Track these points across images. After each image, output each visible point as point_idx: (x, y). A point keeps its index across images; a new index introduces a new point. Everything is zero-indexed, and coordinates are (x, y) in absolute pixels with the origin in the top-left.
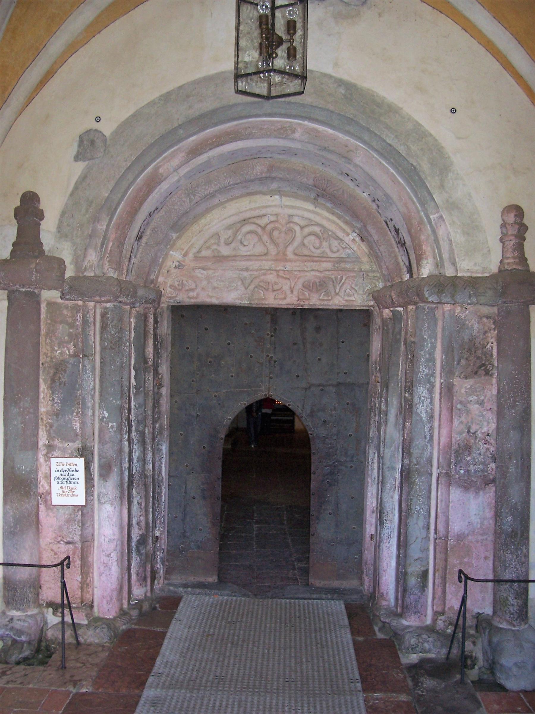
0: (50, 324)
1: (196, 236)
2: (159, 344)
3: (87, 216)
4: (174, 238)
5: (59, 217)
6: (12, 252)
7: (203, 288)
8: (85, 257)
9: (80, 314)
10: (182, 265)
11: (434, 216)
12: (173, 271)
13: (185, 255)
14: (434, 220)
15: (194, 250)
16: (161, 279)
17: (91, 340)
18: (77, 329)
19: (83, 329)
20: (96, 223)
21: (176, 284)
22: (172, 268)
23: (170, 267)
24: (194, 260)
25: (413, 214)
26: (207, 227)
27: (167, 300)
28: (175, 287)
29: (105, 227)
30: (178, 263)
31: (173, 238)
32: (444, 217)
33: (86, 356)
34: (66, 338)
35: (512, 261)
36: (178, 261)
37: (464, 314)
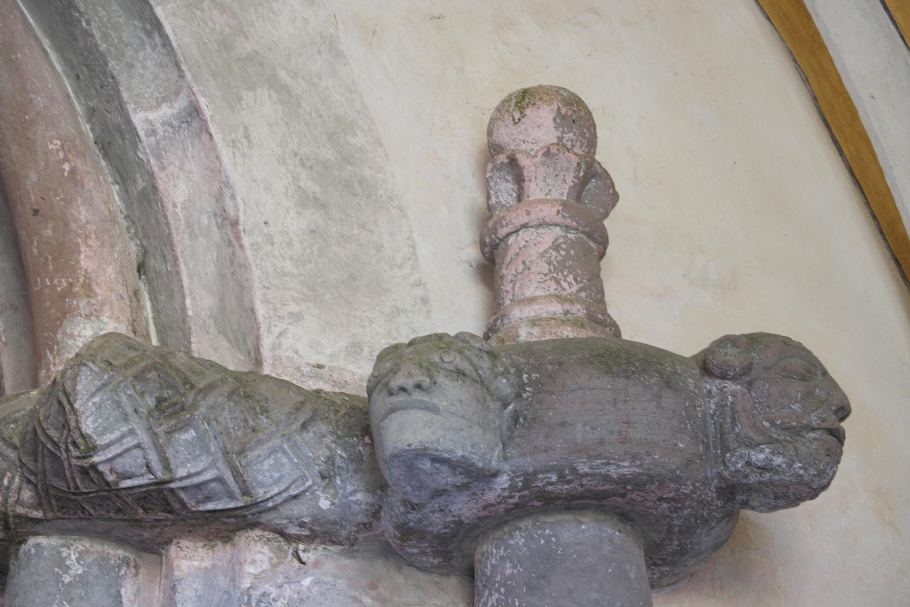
11: (152, 116)
14: (152, 132)
25: (40, 101)
32: (203, 102)
35: (556, 308)
37: (288, 591)
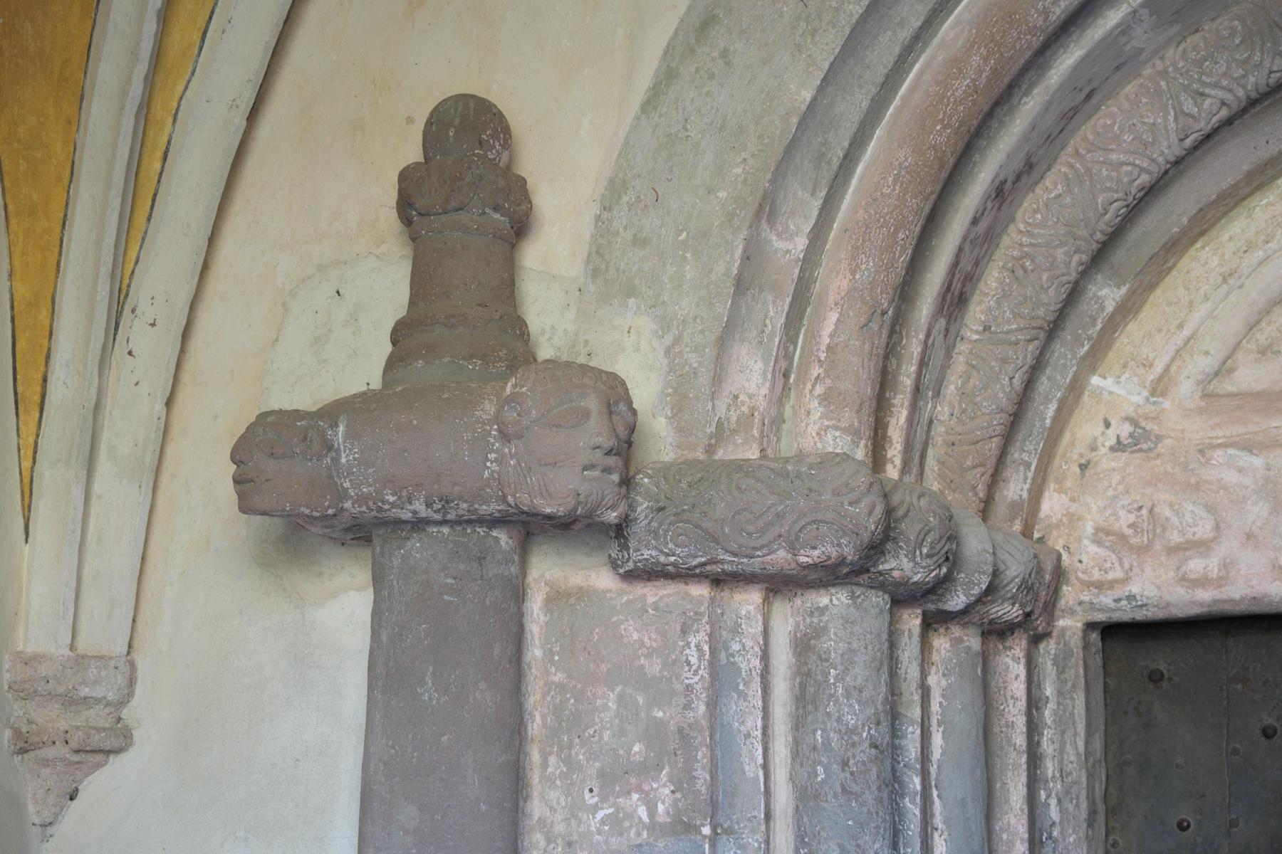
0: (562, 687)
1: (1206, 298)
2: (1053, 802)
3: (722, 195)
4: (1110, 307)
5: (595, 209)
6: (391, 364)
7: (1249, 536)
8: (718, 379)
9: (699, 637)
10: (1146, 435)
12: (1106, 461)
13: (1160, 388)
15: (1201, 364)
16: (1052, 505)
17: (753, 759)
18: (687, 706)
19: (713, 705)
20: (764, 225)
21: (1124, 520)
22: (1103, 451)
23: (1094, 448)
24: (1200, 411)
26: (1260, 254)
27: (1086, 598)
28: (1123, 538)
29: (801, 243)
30: (1127, 429)
31: (1103, 308)
33: (729, 831)
34: (636, 748)
36: (1127, 419)
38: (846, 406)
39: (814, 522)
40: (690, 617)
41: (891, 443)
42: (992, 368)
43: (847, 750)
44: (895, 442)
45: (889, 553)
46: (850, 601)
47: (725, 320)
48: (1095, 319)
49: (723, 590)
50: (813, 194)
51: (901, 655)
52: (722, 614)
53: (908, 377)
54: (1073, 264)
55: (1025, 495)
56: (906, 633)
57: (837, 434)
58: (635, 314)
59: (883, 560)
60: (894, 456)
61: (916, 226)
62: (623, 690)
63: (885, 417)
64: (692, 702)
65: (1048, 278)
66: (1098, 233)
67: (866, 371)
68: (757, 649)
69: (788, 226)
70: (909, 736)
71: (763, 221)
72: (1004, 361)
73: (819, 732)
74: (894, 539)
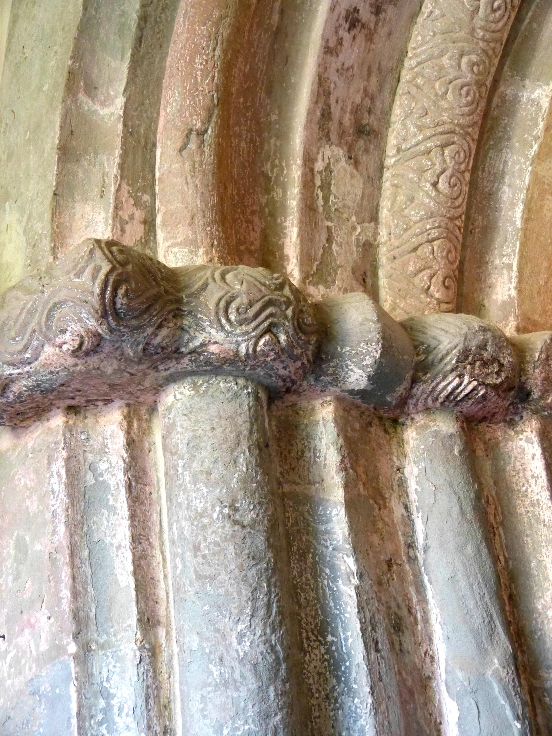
3: (45, 88)
9: (59, 466)
18: (54, 532)
20: (82, 97)
29: (120, 101)
38: (179, 223)
39: (55, 305)
40: (52, 449)
41: (288, 260)
42: (411, 180)
43: (197, 535)
44: (291, 258)
45: (190, 328)
46: (193, 392)
47: (54, 184)
48: (537, 119)
49: (86, 418)
50: (122, 59)
51: (318, 444)
52: (87, 439)
53: (294, 199)
54: (464, 66)
55: (513, 293)
56: (321, 423)
57: (176, 250)
58: (9, 213)
59: (187, 337)
60: (293, 270)
61: (214, 50)
62: (18, 535)
63: (280, 240)
64: (55, 527)
65: (440, 85)
66: (479, 31)
67: (191, 186)
68: (121, 463)
69: (109, 94)
70: (334, 519)
71: (81, 95)
72: (422, 171)
73: (175, 524)
74: (190, 312)
